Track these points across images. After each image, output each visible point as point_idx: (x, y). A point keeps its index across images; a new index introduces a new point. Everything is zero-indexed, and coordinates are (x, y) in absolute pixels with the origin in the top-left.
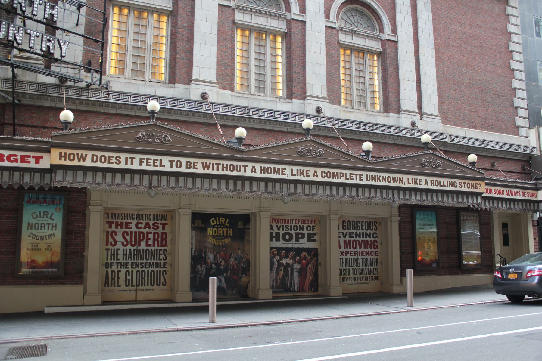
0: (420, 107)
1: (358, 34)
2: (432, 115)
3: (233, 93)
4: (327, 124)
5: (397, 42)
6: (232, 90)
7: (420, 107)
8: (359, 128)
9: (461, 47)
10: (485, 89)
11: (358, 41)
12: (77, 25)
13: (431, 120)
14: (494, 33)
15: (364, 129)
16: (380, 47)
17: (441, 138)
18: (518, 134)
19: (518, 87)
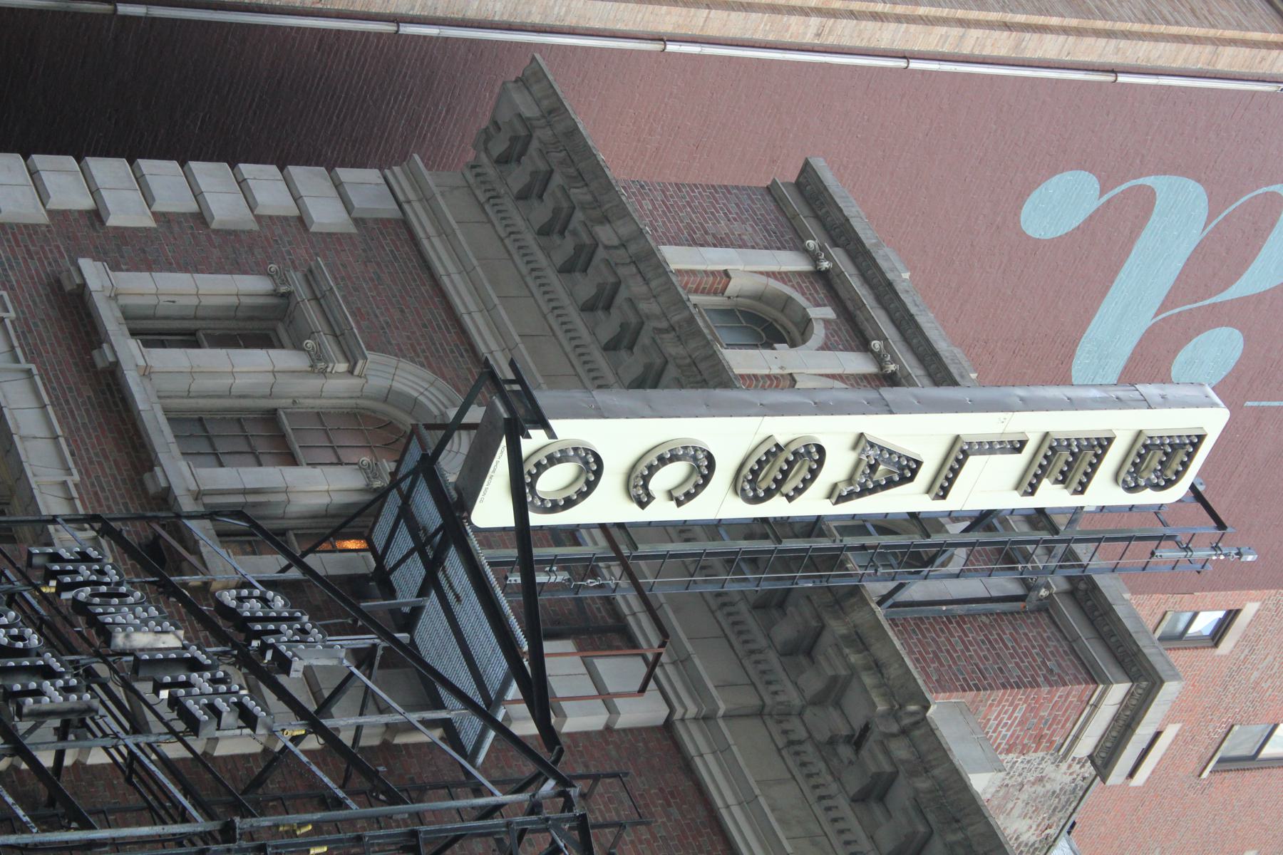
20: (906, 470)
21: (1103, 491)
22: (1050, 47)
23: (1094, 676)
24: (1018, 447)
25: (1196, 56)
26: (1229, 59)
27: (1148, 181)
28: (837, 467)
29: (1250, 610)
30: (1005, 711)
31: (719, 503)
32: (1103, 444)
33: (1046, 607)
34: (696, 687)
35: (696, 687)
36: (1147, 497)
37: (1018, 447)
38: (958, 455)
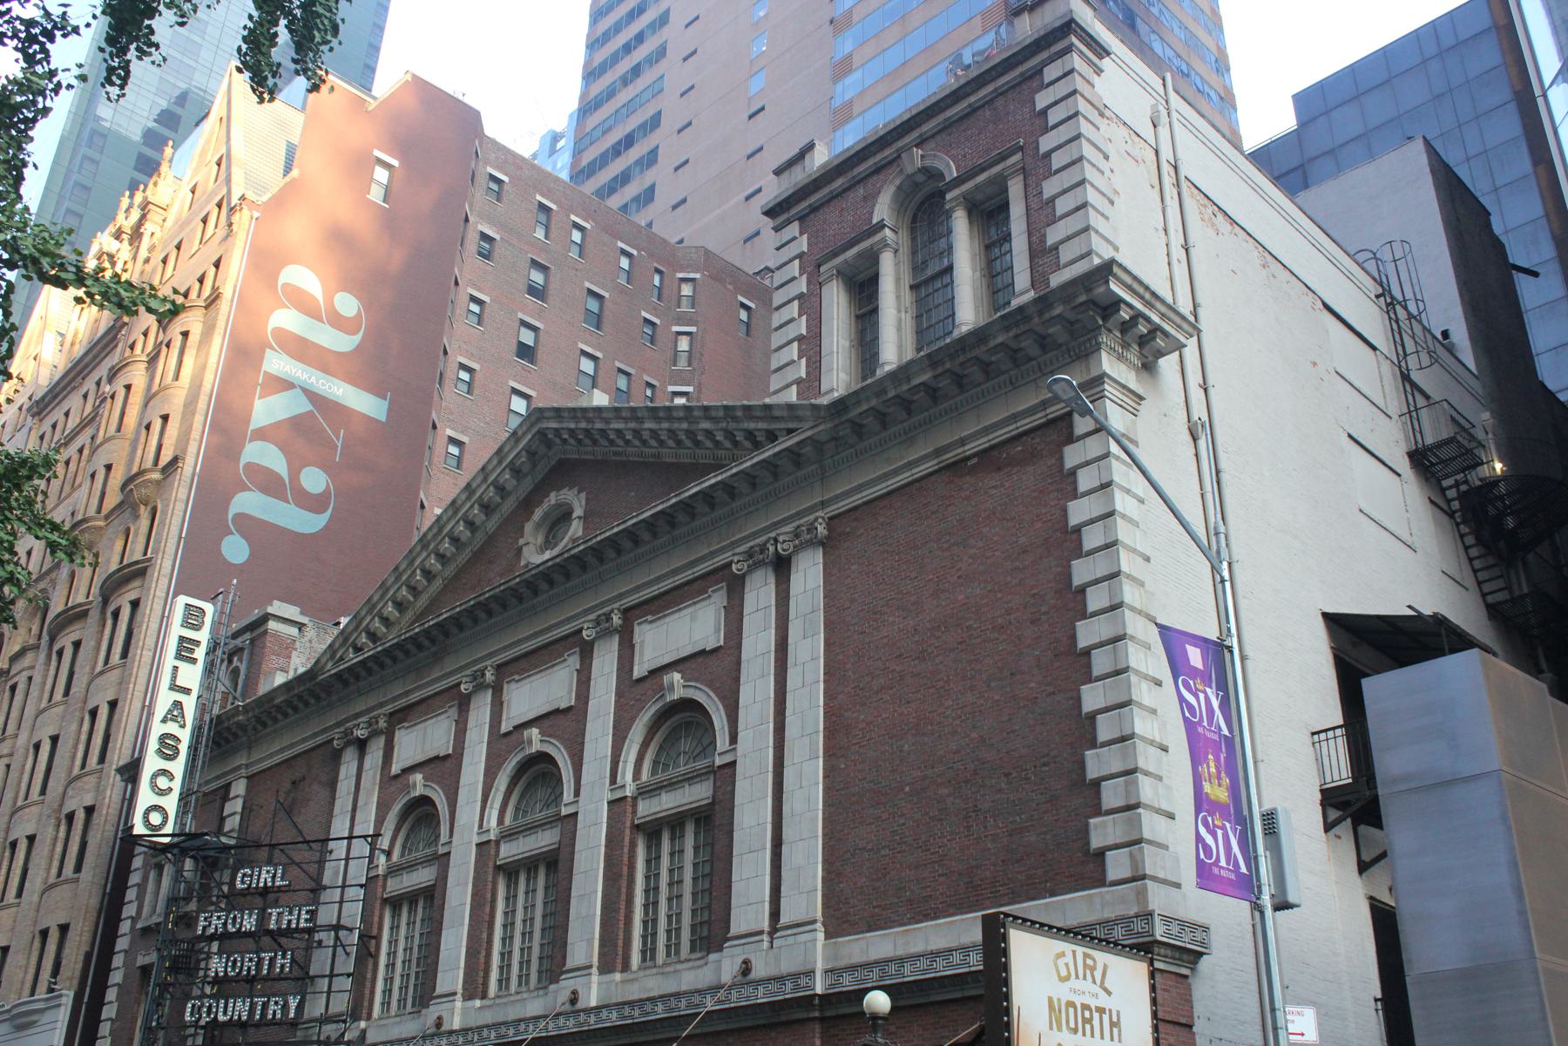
0: (775, 914)
1: (671, 785)
2: (798, 925)
3: (486, 1002)
4: (593, 1022)
5: (734, 762)
6: (484, 996)
7: (775, 914)
8: (625, 1018)
9: (902, 678)
10: (975, 772)
11: (667, 803)
12: (348, 954)
13: (791, 940)
14: (1017, 568)
15: (632, 1017)
16: (710, 793)
17: (797, 988)
18: (1100, 881)
19: (1101, 704)
20: (178, 705)
21: (203, 636)
22: (167, 564)
23: (266, 632)
24: (176, 668)
25: (180, 506)
26: (182, 494)
27: (230, 516)
28: (172, 728)
29: (449, 432)
30: (272, 661)
31: (178, 767)
32: (182, 639)
33: (252, 641)
34: (239, 768)
35: (239, 768)
36: (208, 620)
37: (176, 668)
38: (174, 687)
